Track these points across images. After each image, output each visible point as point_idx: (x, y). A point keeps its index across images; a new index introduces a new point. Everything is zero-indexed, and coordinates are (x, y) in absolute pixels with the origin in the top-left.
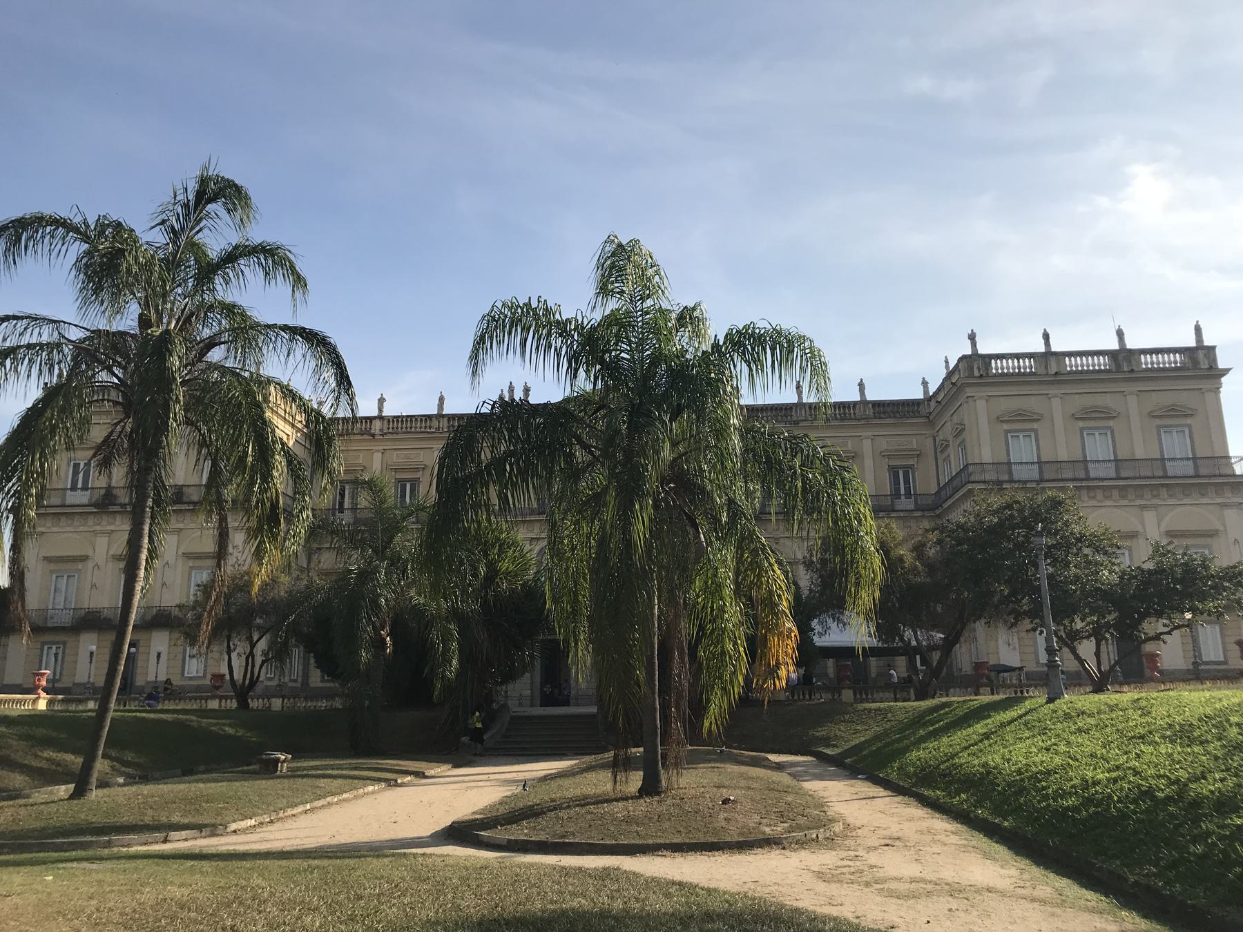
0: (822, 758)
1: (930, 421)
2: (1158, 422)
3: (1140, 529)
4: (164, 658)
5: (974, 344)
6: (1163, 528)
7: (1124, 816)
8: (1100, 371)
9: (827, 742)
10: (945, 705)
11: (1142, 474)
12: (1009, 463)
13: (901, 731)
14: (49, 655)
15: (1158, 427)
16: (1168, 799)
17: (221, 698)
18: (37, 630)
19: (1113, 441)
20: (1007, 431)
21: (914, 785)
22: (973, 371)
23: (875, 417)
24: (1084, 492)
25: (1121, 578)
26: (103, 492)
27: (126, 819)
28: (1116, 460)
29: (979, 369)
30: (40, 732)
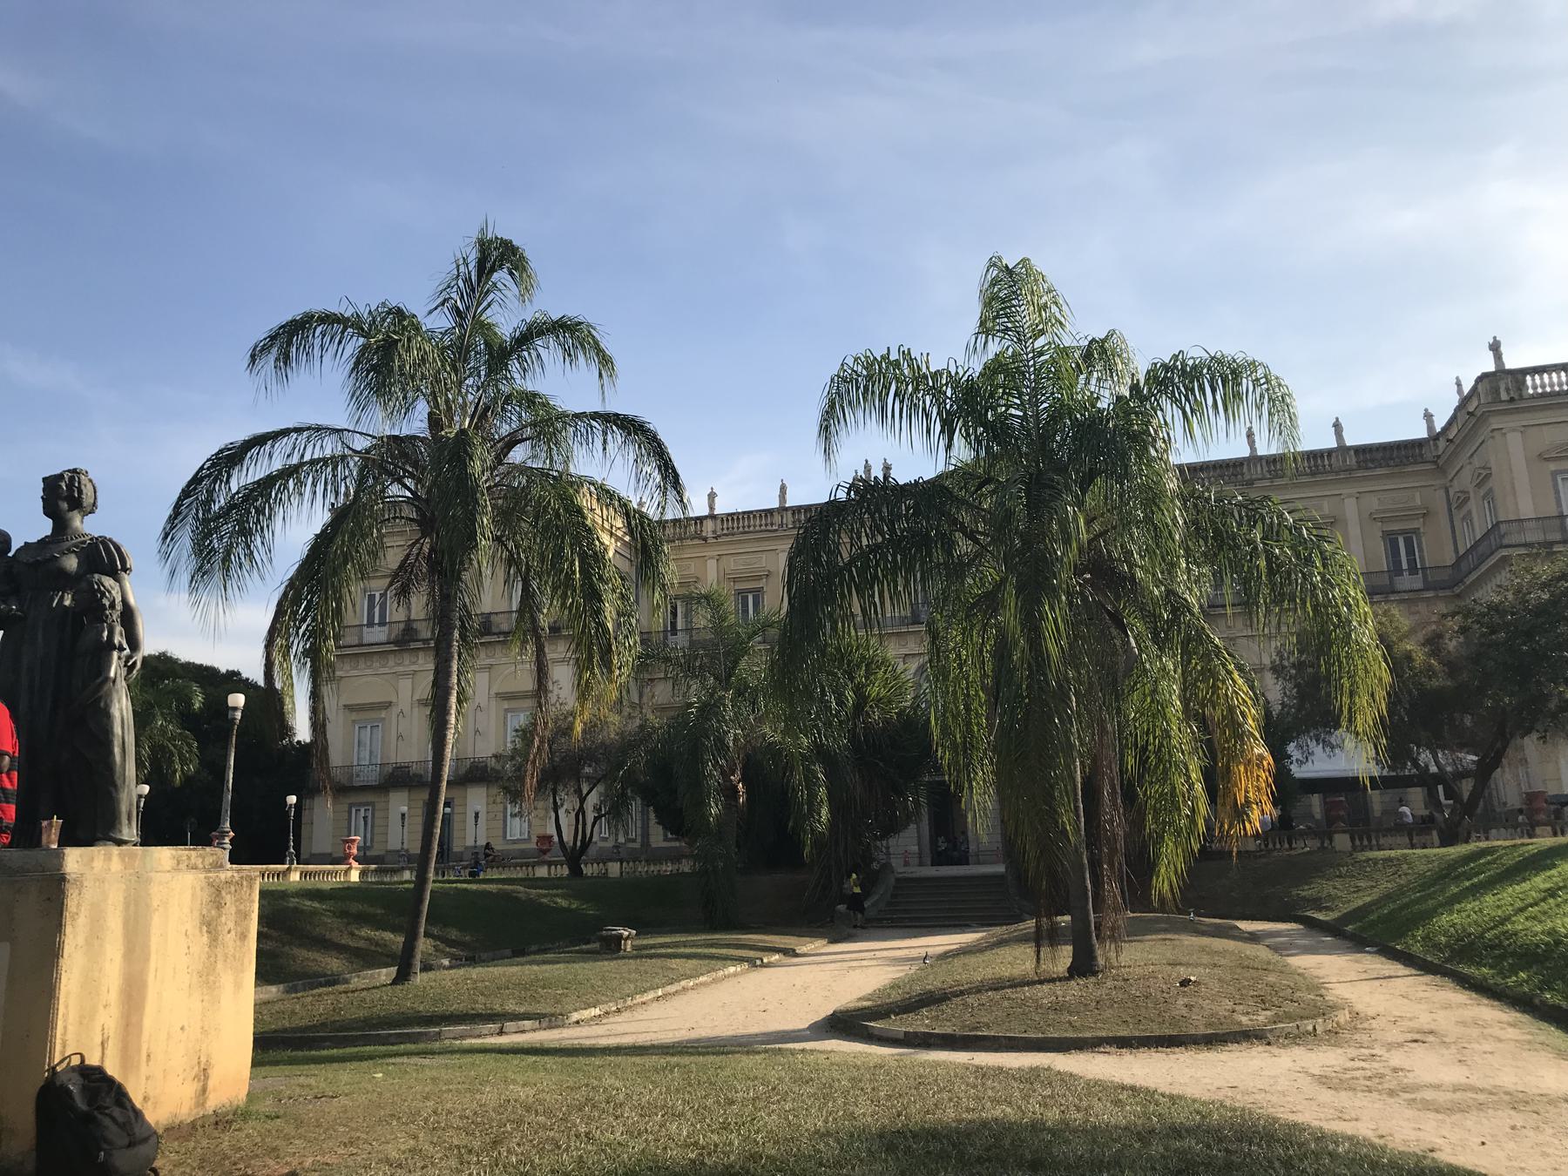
0: (1311, 924)
1: (1440, 467)
4: (482, 817)
5: (1498, 357)
9: (1317, 903)
13: (1423, 887)
17: (550, 864)
18: (342, 790)
20: (1554, 474)
21: (1447, 960)
22: (1500, 394)
23: (1360, 468)
26: (402, 626)
27: (454, 1007)
29: (1507, 390)
30: (356, 907)
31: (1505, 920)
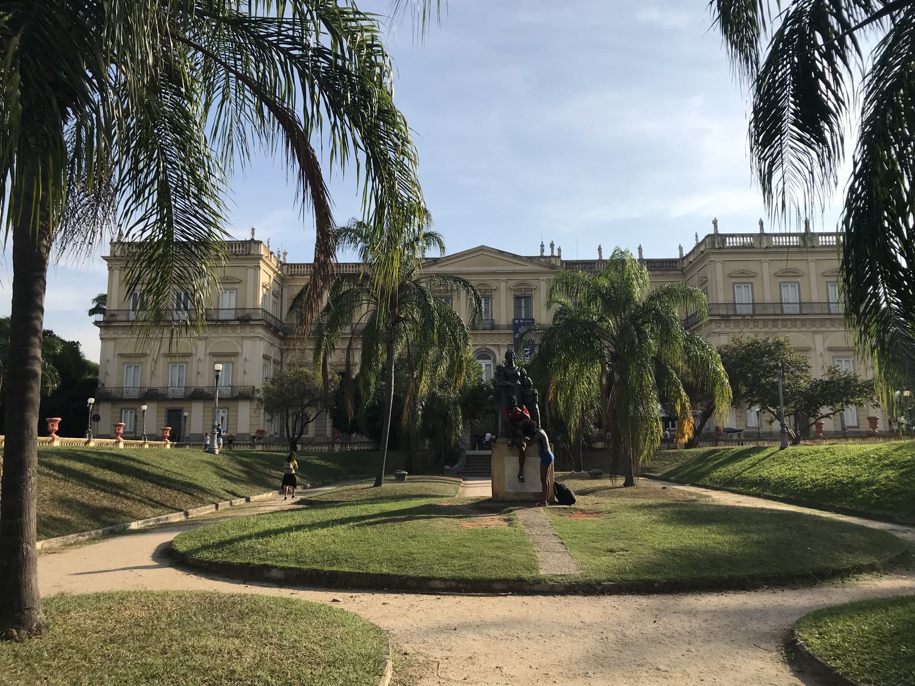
1: (683, 273)
2: (827, 279)
3: (812, 346)
5: (716, 227)
6: (826, 346)
7: (831, 490)
8: (793, 246)
10: (715, 451)
11: (817, 311)
12: (735, 304)
13: (695, 463)
14: (129, 416)
15: (827, 282)
16: (848, 483)
17: (263, 444)
19: (799, 290)
20: (734, 283)
22: (714, 244)
24: (780, 323)
25: (811, 386)
28: (800, 303)
31: (739, 474)
